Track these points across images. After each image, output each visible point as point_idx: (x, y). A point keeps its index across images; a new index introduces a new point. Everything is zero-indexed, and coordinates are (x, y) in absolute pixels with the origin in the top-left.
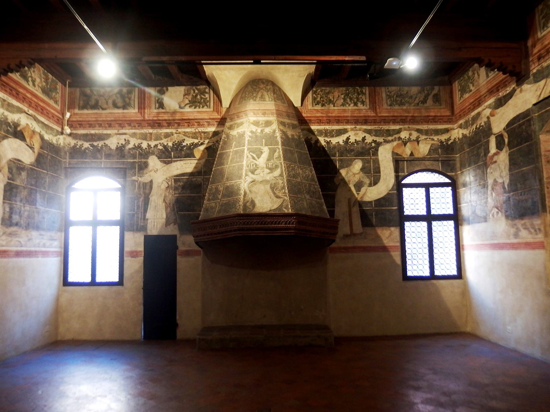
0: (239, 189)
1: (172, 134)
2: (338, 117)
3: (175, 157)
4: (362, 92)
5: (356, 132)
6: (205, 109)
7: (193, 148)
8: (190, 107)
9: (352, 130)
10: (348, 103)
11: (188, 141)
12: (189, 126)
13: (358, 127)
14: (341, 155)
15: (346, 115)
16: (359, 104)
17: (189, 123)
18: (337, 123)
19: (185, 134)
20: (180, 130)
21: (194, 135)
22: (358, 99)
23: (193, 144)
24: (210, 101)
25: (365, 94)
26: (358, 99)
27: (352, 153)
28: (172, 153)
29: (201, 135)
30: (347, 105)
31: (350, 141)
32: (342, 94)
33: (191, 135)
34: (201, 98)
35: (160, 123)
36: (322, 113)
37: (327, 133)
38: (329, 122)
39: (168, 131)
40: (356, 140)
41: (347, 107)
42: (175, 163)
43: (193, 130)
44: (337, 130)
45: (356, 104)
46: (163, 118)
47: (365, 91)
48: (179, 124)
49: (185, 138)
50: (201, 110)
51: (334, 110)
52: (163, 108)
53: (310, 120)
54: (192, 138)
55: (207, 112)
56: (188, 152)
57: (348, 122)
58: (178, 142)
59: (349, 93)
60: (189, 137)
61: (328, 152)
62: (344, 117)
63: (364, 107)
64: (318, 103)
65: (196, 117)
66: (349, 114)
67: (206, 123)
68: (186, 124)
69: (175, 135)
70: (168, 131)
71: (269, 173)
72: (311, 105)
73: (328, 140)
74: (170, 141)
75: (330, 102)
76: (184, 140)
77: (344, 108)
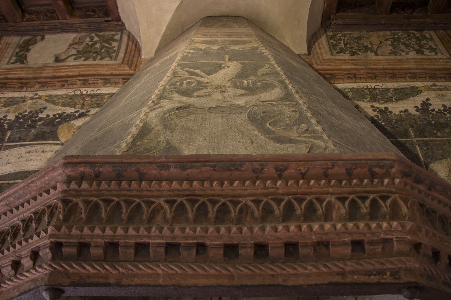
0: (127, 127)
1: (24, 100)
2: (391, 69)
3: (10, 140)
4: (425, 37)
5: (440, 92)
6: (107, 61)
7: (60, 123)
8: (75, 59)
9: (428, 88)
10: (403, 51)
11: (53, 111)
12: (63, 86)
13: (440, 84)
14: (421, 132)
15: (406, 66)
16: (426, 52)
17: (67, 81)
18: (391, 77)
19: (51, 100)
20: (40, 93)
21: (70, 101)
22: (421, 46)
23: (60, 115)
24: (118, 51)
25: (431, 39)
26: (421, 46)
27: (447, 130)
28: (9, 133)
29: (84, 99)
30: (403, 54)
31: (431, 108)
32: (387, 40)
33: (61, 100)
34: (103, 47)
35: (5, 83)
36: (354, 64)
37: (373, 95)
38: (374, 77)
39: (17, 95)
40: (444, 106)
41: (403, 56)
42: (7, 151)
43: (70, 92)
44: (395, 89)
45: (418, 52)
46: (17, 76)
47: (431, 36)
48: (44, 85)
49: (48, 105)
50: (97, 62)
51: (378, 60)
52: (22, 62)
53: (330, 74)
54: (64, 105)
55: (107, 65)
56: (45, 129)
57: (414, 77)
58: (30, 112)
59: (399, 40)
60: (56, 104)
61: (388, 128)
62: (401, 69)
63: (439, 56)
64: (342, 51)
65: (82, 73)
66: (412, 66)
67: (100, 81)
68: (58, 84)
69: (30, 102)
70: (17, 95)
71: (243, 95)
72: (329, 53)
73: (382, 106)
74: (14, 112)
75: (366, 49)
76: (45, 108)
77: (398, 57)
